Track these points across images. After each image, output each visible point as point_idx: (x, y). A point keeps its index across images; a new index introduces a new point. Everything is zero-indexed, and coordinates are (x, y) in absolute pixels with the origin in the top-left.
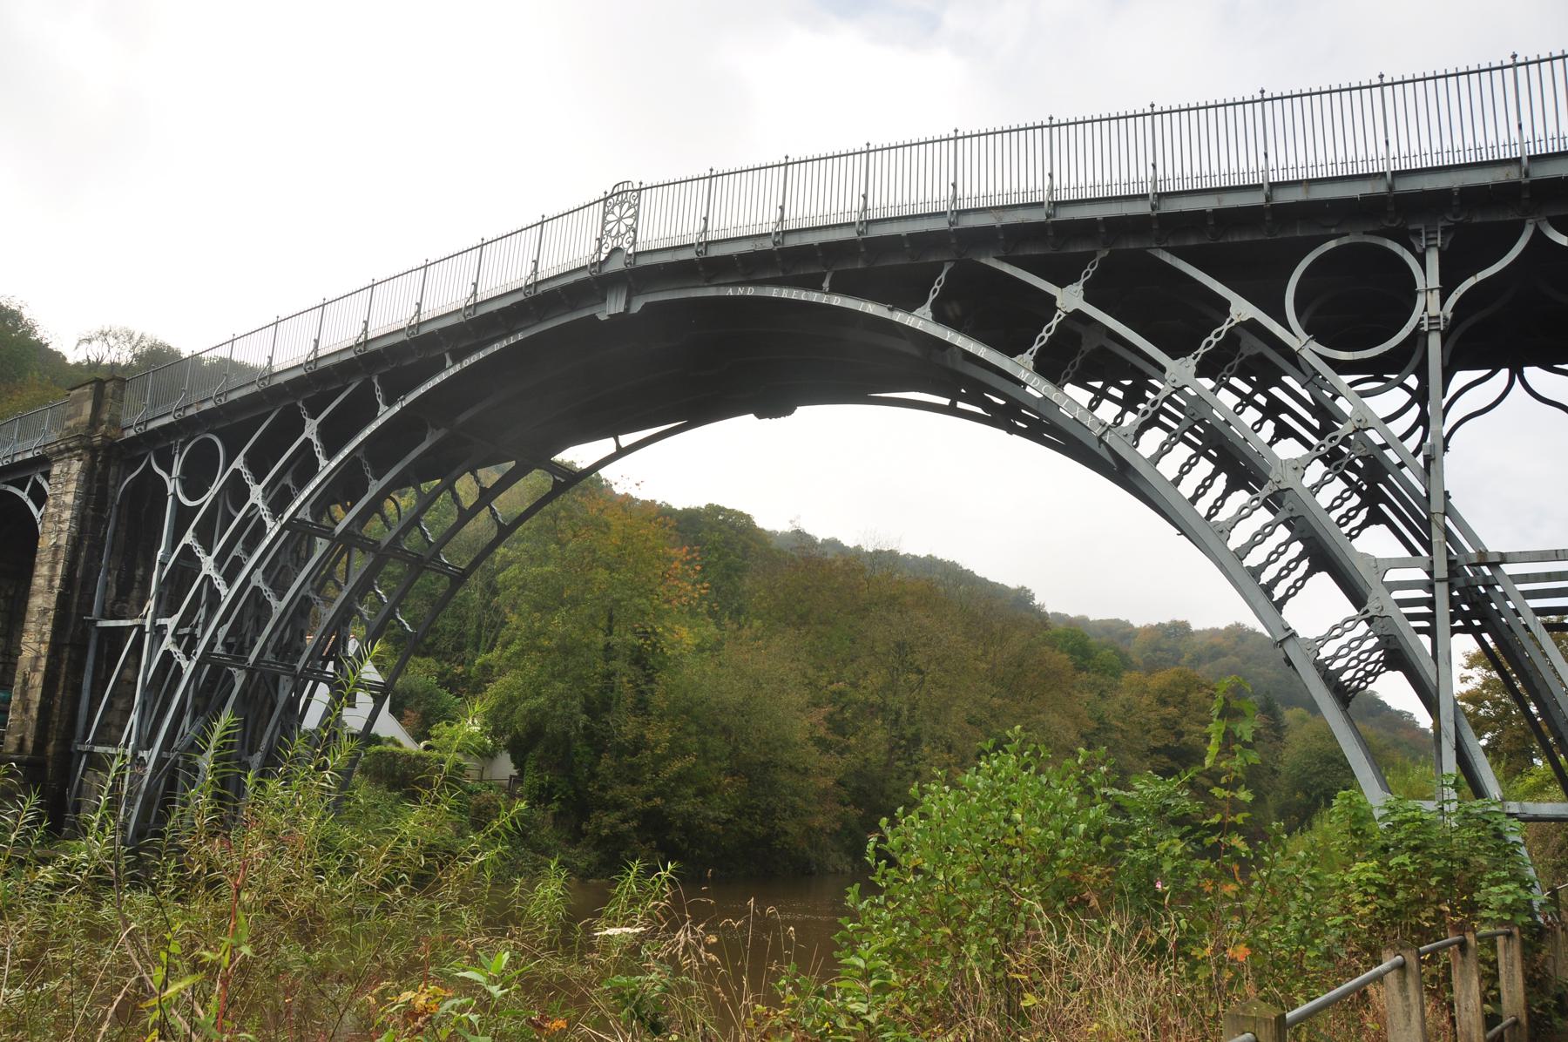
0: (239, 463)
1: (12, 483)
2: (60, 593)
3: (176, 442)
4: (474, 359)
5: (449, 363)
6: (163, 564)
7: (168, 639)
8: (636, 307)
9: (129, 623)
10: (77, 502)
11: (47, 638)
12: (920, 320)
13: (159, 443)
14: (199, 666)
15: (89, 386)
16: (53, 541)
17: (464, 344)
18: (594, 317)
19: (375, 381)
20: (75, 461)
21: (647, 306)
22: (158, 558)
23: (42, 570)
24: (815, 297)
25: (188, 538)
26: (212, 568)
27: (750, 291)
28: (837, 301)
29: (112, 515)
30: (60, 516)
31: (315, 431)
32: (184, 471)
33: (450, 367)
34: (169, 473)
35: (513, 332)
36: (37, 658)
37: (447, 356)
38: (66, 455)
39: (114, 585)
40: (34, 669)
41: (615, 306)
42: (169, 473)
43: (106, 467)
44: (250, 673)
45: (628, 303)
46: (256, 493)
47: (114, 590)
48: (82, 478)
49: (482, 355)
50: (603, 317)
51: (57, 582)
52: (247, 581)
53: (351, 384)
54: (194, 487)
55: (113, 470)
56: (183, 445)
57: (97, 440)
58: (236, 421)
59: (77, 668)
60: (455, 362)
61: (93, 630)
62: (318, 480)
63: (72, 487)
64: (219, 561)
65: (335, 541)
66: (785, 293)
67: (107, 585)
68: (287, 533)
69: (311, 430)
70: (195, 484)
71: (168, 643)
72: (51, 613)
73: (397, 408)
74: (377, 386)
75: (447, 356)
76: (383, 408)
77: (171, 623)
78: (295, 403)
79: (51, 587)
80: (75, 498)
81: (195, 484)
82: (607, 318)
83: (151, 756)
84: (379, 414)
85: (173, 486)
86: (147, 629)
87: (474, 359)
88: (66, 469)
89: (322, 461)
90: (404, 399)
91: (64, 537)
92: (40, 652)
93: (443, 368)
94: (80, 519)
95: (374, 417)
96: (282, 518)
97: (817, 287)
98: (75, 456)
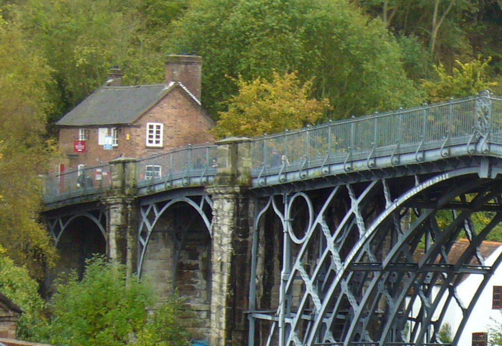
0: (320, 219)
1: (192, 198)
2: (227, 296)
3: (285, 194)
4: (429, 183)
5: (417, 183)
6: (285, 282)
7: (292, 333)
8: (494, 176)
9: (269, 318)
10: (231, 232)
11: (224, 326)
13: (278, 193)
15: (228, 146)
16: (220, 258)
17: (423, 172)
18: (476, 176)
19: (384, 182)
20: (225, 201)
21: (499, 175)
22: (282, 278)
23: (216, 278)
25: (298, 266)
26: (311, 289)
29: (252, 238)
30: (221, 242)
31: (357, 208)
32: (291, 216)
33: (418, 186)
34: (283, 213)
36: (219, 339)
37: (416, 177)
38: (220, 196)
39: (261, 285)
41: (483, 174)
42: (283, 213)
45: (490, 172)
46: (331, 240)
48: (231, 214)
49: (431, 184)
51: (225, 288)
52: (338, 288)
53: (372, 181)
54: (299, 231)
55: (251, 206)
56: (289, 197)
57: (237, 189)
58: (317, 188)
61: (250, 319)
62: (359, 244)
63: (227, 221)
64: (318, 282)
65: (383, 272)
67: (257, 287)
68: (351, 273)
69: (355, 204)
70: (299, 228)
72: (224, 310)
73: (394, 207)
74: (385, 188)
75: (416, 177)
76: (388, 203)
77: (293, 322)
78: (345, 186)
79: (222, 291)
80: (229, 230)
81: (299, 228)
84: (387, 207)
85: (287, 226)
86: (280, 326)
87: (429, 183)
88: (221, 207)
89: (361, 232)
90: (397, 201)
91: (225, 260)
92: (219, 335)
93: (412, 186)
94: (234, 243)
95: (382, 209)
96: (344, 265)
98: (226, 198)
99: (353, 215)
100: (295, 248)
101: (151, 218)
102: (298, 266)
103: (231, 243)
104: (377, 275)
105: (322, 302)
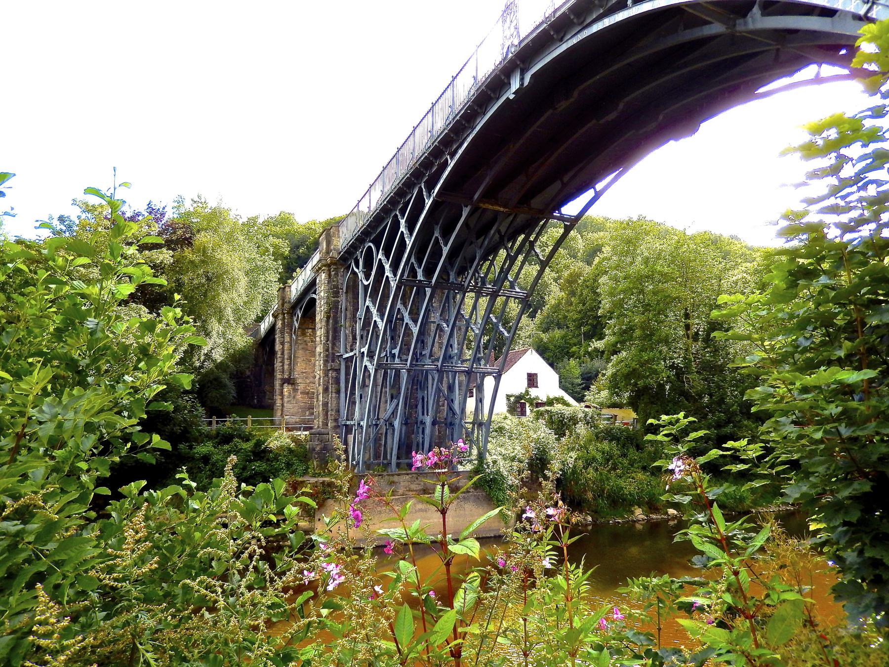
4: (460, 152)
5: (449, 161)
6: (360, 319)
8: (527, 81)
14: (376, 370)
18: (508, 98)
19: (423, 187)
40: (319, 385)
43: (337, 274)
44: (409, 371)
45: (522, 79)
47: (351, 337)
50: (512, 97)
59: (337, 381)
66: (607, 22)
71: (366, 361)
76: (427, 201)
77: (365, 350)
82: (514, 96)
83: (364, 423)
85: (361, 275)
99: (402, 232)
100: (366, 288)
101: (297, 320)
102: (368, 303)
103: (327, 303)
104: (428, 291)
105: (383, 321)
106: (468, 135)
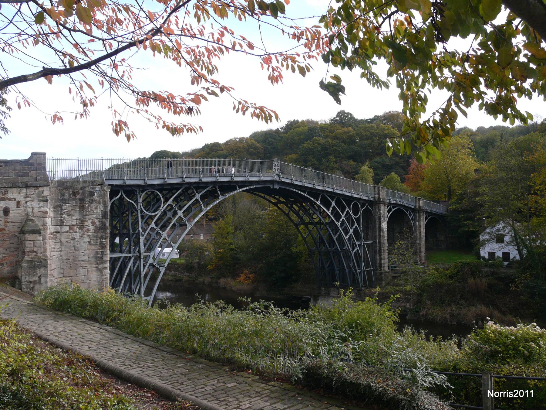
5: (238, 188)
12: (318, 203)
24: (305, 195)
27: (296, 191)
28: (308, 197)
35: (254, 185)
41: (277, 187)
42: (136, 202)
50: (272, 187)
60: (240, 188)
66: (301, 193)
69: (198, 196)
73: (224, 197)
85: (140, 206)
93: (236, 189)
97: (305, 193)
106: (250, 186)
